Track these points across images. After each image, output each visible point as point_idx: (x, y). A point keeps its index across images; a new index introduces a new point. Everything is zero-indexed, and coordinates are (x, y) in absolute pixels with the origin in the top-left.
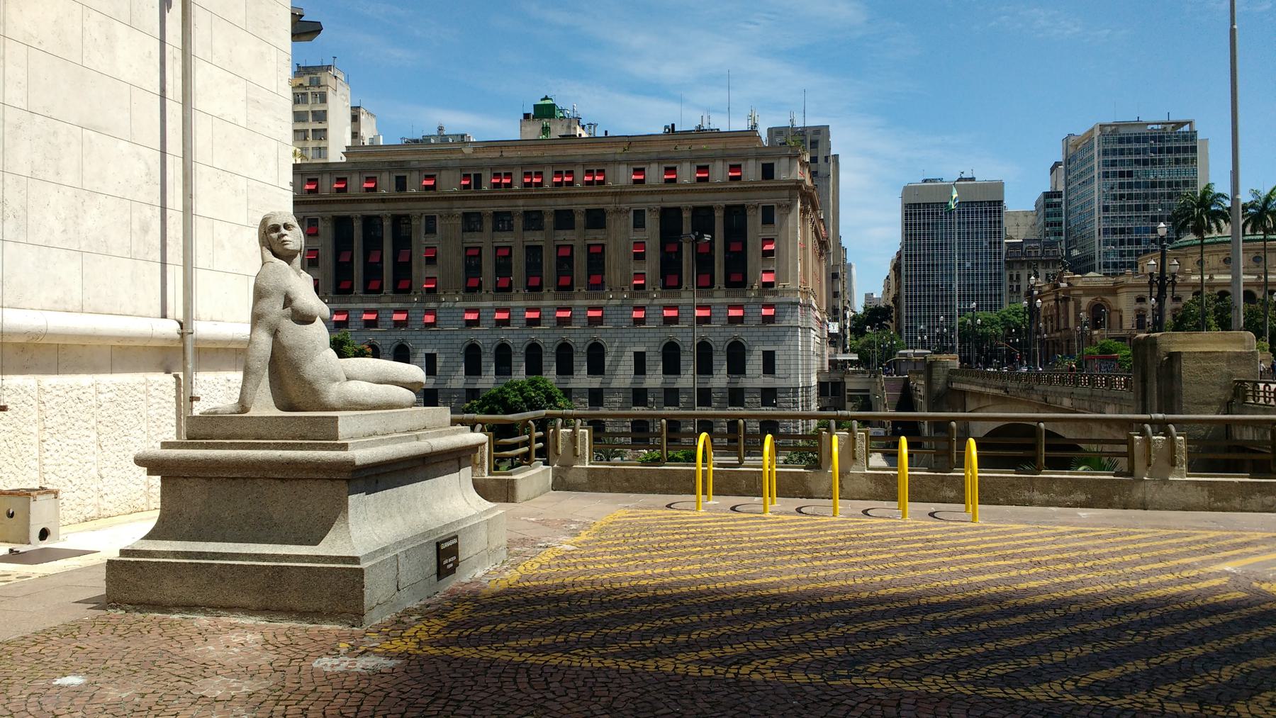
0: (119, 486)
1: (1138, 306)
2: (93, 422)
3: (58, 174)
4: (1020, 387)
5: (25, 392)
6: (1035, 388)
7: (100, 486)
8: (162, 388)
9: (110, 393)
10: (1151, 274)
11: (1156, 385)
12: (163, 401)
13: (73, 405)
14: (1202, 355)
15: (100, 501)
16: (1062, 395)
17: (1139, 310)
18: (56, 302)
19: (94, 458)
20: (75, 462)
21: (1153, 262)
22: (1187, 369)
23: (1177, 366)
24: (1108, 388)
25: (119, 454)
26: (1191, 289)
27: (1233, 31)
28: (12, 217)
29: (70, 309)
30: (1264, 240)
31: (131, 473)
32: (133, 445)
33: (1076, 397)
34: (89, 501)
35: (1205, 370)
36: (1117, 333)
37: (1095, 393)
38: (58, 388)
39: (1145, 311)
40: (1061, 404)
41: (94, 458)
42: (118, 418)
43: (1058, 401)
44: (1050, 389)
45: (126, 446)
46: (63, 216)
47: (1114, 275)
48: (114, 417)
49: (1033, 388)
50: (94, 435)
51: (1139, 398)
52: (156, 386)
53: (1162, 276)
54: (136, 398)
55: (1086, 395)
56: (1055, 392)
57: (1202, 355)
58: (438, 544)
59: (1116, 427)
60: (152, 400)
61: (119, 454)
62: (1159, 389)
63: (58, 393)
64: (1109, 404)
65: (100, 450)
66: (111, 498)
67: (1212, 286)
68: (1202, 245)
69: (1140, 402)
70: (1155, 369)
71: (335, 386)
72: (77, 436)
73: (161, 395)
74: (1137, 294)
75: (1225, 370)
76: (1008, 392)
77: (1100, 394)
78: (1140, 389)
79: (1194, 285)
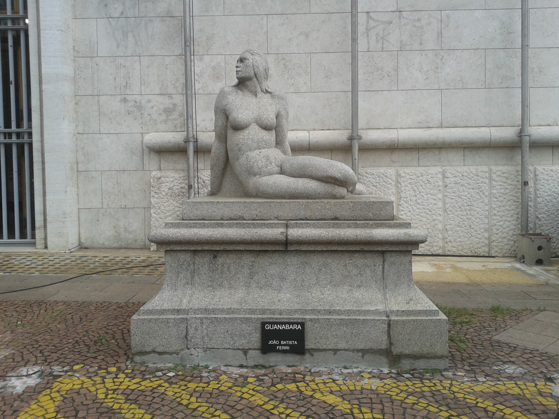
0: (463, 237)
2: (440, 196)
3: (421, 44)
5: (386, 176)
7: (446, 236)
8: (505, 175)
9: (456, 178)
12: (506, 184)
13: (423, 184)
15: (446, 245)
18: (420, 123)
19: (440, 218)
20: (424, 219)
25: (462, 217)
28: (386, 76)
29: (431, 126)
31: (472, 231)
32: (475, 212)
34: (436, 244)
38: (410, 174)
41: (440, 218)
42: (462, 194)
45: (468, 212)
46: (425, 69)
48: (458, 193)
50: (440, 204)
52: (499, 173)
54: (478, 182)
58: (263, 324)
60: (494, 183)
61: (462, 217)
63: (411, 177)
65: (445, 214)
66: (454, 244)
71: (254, 179)
72: (426, 204)
73: (504, 180)
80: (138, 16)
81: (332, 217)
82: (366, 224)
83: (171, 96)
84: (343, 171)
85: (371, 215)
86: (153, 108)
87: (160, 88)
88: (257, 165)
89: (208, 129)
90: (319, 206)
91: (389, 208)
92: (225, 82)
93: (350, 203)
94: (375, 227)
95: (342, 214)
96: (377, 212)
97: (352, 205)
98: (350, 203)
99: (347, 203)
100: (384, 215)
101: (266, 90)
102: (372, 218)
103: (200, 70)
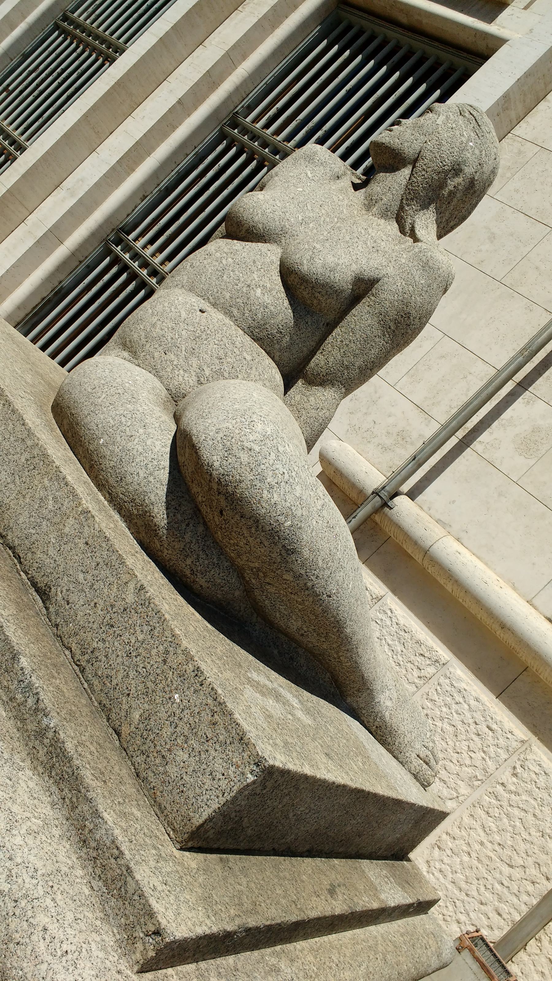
80: (499, 280)
81: (38, 579)
82: (31, 702)
83: (429, 421)
84: (244, 457)
85: (136, 715)
86: (390, 416)
87: (426, 398)
88: (154, 325)
89: (432, 512)
90: (55, 499)
91: (218, 766)
92: (531, 464)
93: (131, 586)
94: (42, 752)
95: (73, 598)
96: (167, 731)
97: (130, 598)
98: (131, 586)
99: (125, 577)
100: (172, 770)
101: (413, 229)
102: (125, 730)
103: (512, 417)
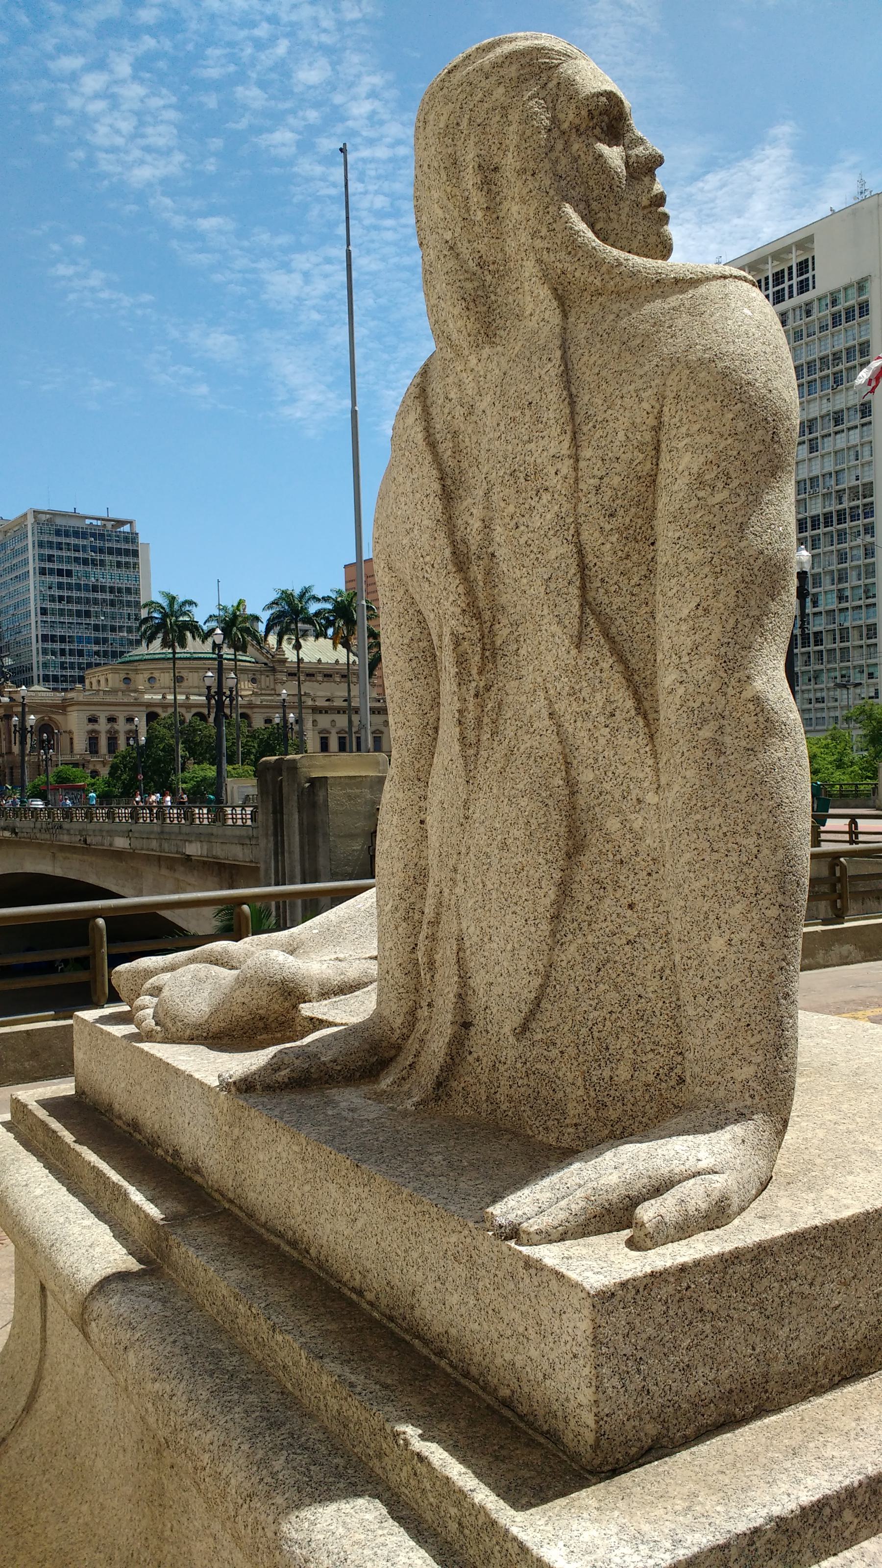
1: (91, 727)
4: (38, 825)
6: (66, 826)
10: (209, 688)
11: (296, 816)
14: (347, 781)
16: (111, 833)
17: (93, 731)
21: (210, 674)
22: (334, 792)
23: (321, 794)
24: (188, 823)
26: (144, 708)
27: (354, 413)
30: (235, 660)
33: (136, 835)
35: (350, 797)
36: (68, 758)
37: (167, 830)
39: (117, 732)
40: (111, 845)
43: (107, 842)
44: (90, 826)
47: (65, 690)
49: (61, 827)
51: (270, 832)
53: (220, 693)
55: (152, 832)
56: (101, 831)
57: (347, 781)
59: (182, 869)
62: (301, 824)
64: (190, 842)
67: (188, 706)
68: (174, 659)
69: (272, 839)
70: (296, 798)
74: (107, 714)
75: (369, 796)
76: (16, 834)
77: (176, 829)
78: (271, 821)
79: (148, 705)
